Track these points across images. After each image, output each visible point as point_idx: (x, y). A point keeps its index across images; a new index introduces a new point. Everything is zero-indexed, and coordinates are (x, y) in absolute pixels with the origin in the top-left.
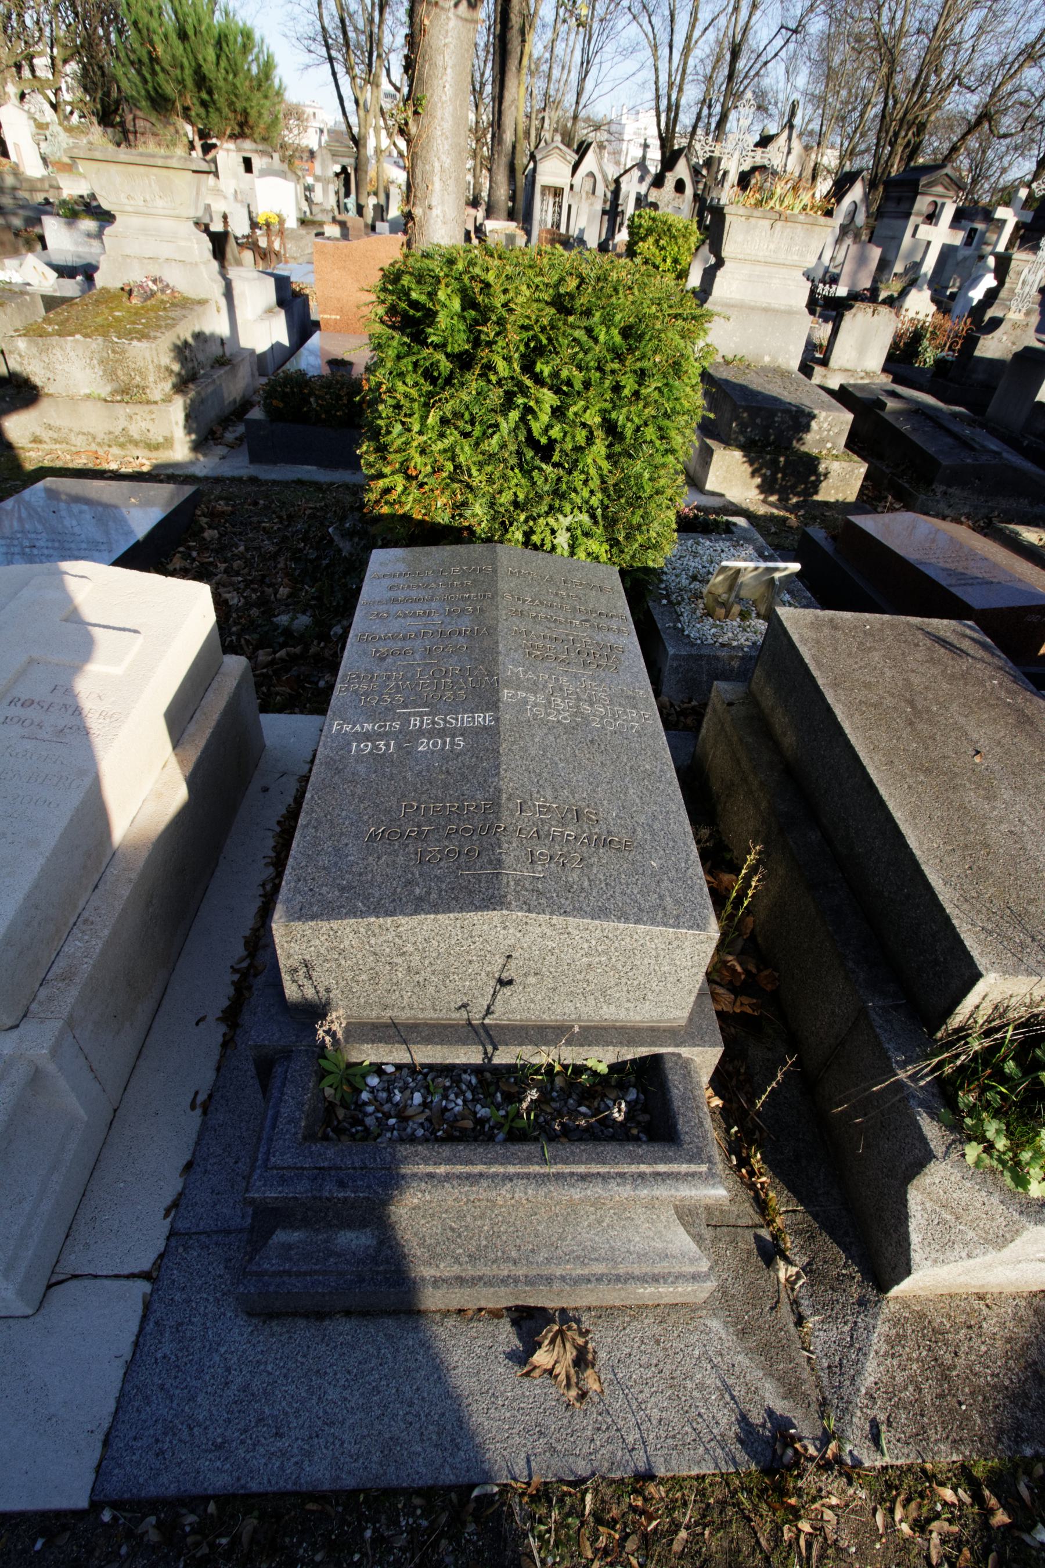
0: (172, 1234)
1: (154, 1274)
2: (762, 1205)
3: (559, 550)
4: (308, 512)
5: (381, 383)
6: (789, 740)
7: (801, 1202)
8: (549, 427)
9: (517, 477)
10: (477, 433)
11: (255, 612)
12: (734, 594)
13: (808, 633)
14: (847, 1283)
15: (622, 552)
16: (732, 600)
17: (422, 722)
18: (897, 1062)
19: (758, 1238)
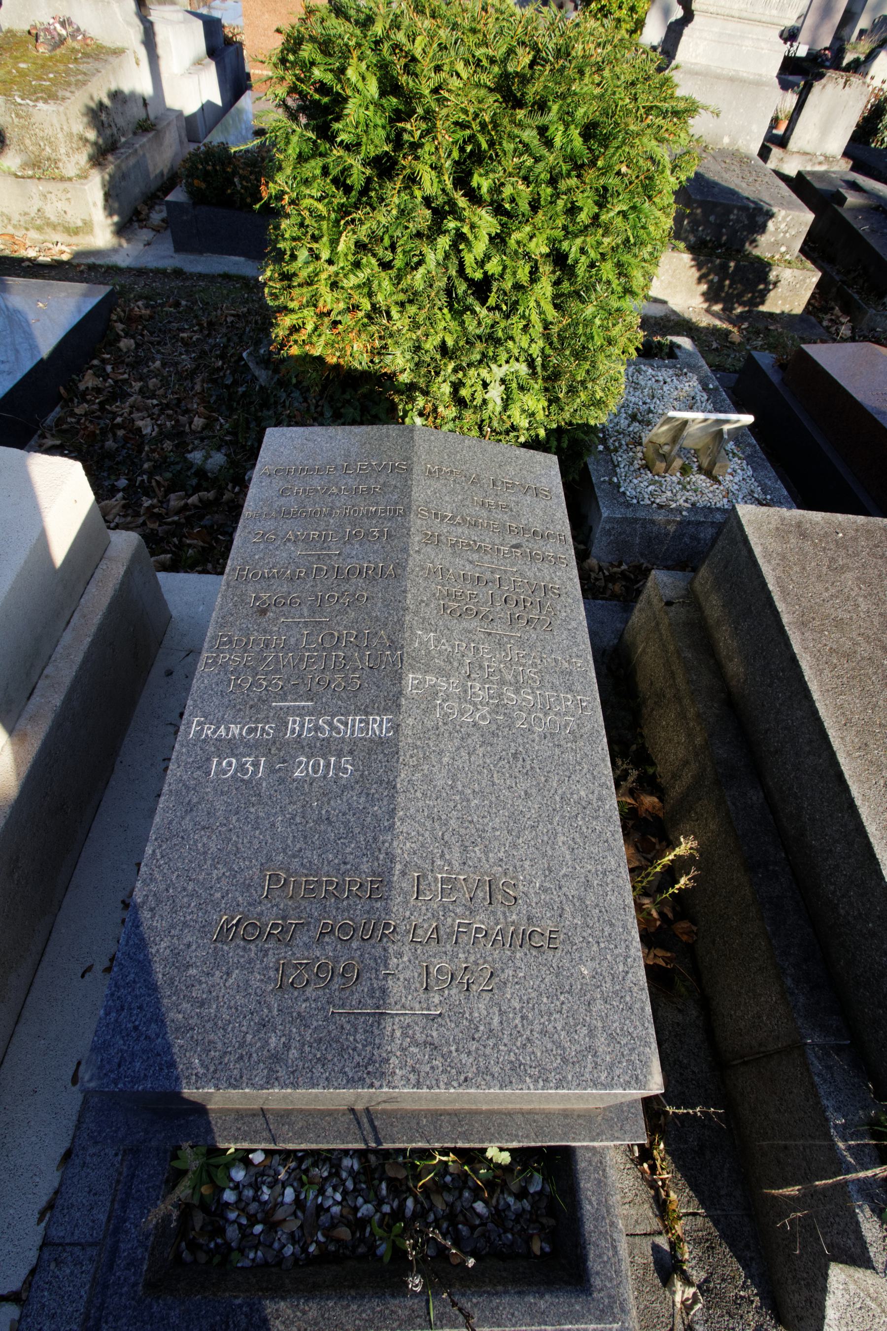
0: (46, 1243)
1: (24, 1297)
2: (662, 1207)
3: (490, 406)
4: (229, 319)
5: (283, 193)
6: (735, 668)
7: (702, 1203)
8: (488, 257)
9: (445, 319)
10: (398, 263)
11: (168, 445)
12: (677, 447)
13: (774, 545)
14: (745, 1308)
15: (562, 410)
16: (674, 454)
17: (302, 726)
18: (836, 1125)
19: (656, 1248)
